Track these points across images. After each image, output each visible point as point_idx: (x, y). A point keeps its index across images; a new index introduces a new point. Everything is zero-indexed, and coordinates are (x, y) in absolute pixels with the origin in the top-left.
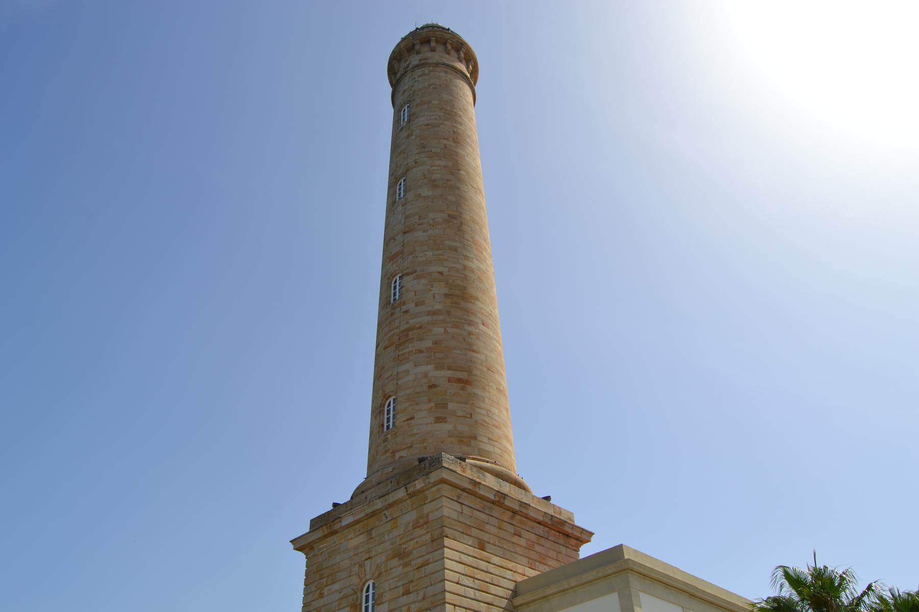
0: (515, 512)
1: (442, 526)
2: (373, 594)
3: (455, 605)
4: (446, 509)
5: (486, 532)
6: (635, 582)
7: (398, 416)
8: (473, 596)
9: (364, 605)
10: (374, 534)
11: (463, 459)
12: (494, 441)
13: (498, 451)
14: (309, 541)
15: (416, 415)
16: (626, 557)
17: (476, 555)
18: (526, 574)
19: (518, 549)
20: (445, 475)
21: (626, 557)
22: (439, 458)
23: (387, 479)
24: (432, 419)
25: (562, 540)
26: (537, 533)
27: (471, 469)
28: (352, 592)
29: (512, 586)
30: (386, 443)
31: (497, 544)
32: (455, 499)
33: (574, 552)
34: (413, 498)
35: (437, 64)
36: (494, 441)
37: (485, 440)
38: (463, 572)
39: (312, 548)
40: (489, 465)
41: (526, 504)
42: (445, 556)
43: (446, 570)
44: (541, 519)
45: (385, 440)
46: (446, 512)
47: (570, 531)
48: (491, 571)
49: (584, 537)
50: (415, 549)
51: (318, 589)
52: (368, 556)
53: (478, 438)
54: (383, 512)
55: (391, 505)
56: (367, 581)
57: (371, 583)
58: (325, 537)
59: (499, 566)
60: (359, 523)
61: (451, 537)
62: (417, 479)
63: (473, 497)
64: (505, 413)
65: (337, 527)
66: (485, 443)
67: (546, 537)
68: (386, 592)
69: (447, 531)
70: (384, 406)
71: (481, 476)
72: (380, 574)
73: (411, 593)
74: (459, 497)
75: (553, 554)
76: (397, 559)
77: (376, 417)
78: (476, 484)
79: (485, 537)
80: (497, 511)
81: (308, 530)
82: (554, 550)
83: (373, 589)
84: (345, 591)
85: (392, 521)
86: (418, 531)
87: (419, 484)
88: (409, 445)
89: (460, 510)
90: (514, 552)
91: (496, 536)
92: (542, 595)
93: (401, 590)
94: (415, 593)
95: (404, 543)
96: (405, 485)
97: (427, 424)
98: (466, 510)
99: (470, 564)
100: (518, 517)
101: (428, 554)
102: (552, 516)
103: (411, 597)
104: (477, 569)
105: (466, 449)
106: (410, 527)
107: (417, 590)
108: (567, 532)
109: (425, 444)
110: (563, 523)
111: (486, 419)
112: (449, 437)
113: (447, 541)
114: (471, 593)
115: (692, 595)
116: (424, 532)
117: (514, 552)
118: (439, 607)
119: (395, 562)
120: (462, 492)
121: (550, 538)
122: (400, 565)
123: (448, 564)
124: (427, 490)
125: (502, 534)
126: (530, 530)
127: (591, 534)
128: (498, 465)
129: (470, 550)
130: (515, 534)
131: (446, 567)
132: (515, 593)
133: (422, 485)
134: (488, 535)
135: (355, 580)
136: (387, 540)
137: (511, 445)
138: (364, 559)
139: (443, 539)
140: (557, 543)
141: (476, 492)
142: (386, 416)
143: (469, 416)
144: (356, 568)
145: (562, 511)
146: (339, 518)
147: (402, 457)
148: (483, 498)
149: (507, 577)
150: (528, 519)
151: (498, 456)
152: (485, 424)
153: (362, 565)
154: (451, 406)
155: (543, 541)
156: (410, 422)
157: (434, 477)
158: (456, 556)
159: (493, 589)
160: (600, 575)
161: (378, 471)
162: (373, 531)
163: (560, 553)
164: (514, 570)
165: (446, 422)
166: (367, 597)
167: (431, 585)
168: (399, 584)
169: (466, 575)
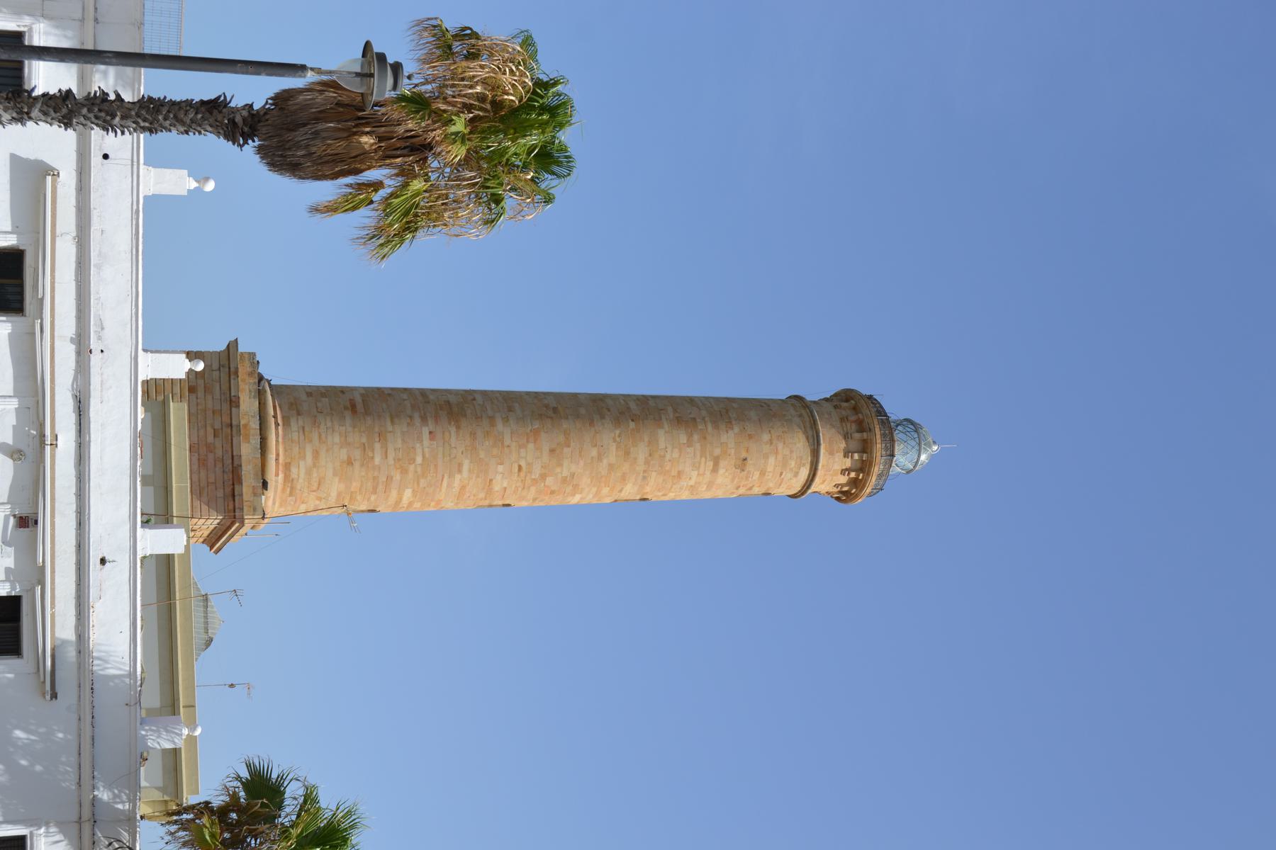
27: (255, 383)
35: (806, 405)
37: (301, 423)
40: (271, 412)
53: (299, 417)
74: (223, 366)
79: (201, 393)
98: (216, 374)
113: (246, 517)
130: (214, 429)
155: (219, 465)
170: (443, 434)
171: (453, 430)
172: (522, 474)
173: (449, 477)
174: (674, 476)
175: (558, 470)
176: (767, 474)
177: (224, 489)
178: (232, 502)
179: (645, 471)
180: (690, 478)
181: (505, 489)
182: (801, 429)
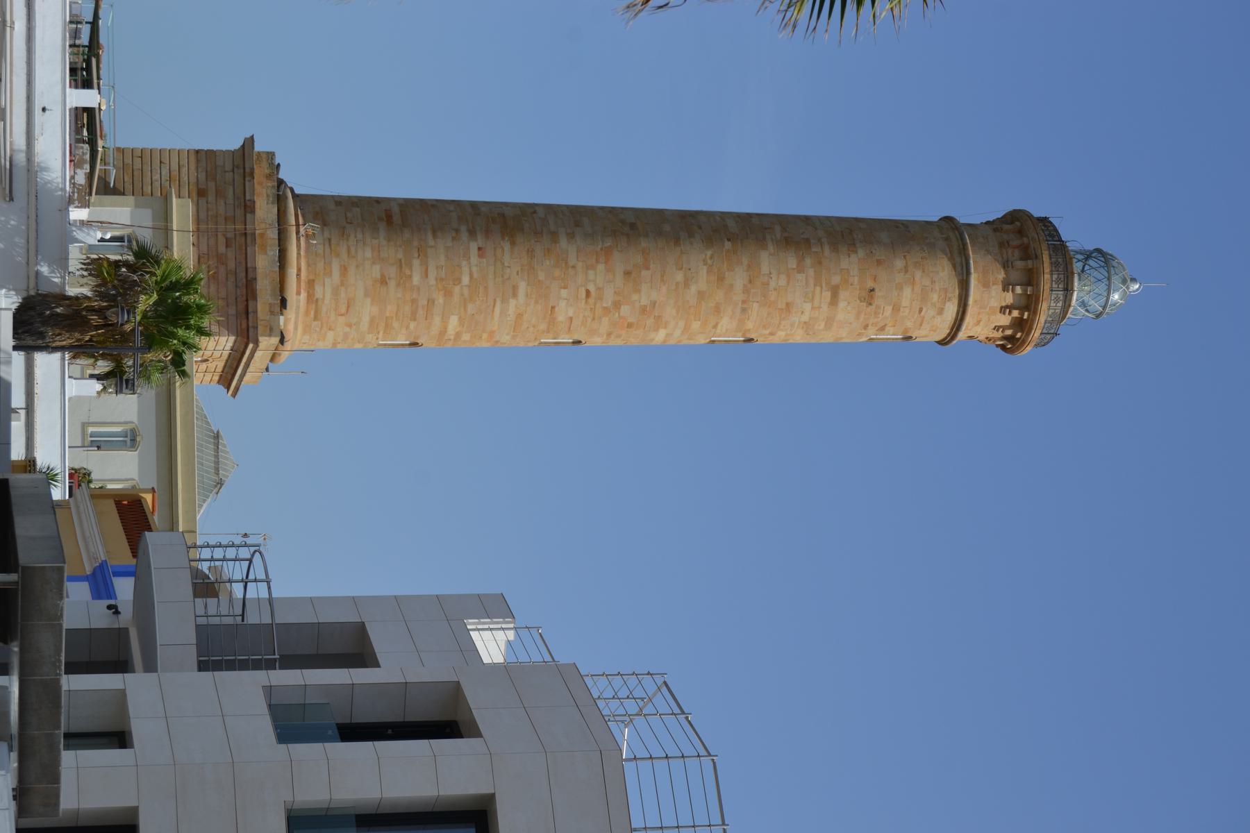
8: (154, 178)
27: (273, 187)
40: (292, 220)
53: (325, 228)
74: (238, 167)
79: (211, 198)
98: (229, 176)
104: (179, 186)
114: (156, 177)
129: (193, 180)
130: (226, 239)
140: (236, 302)
170: (495, 249)
171: (507, 246)
172: (591, 301)
173: (502, 303)
174: (781, 309)
175: (635, 297)
176: (902, 309)
177: (237, 306)
178: (246, 321)
179: (744, 302)
180: (802, 312)
181: (571, 318)
182: (946, 255)
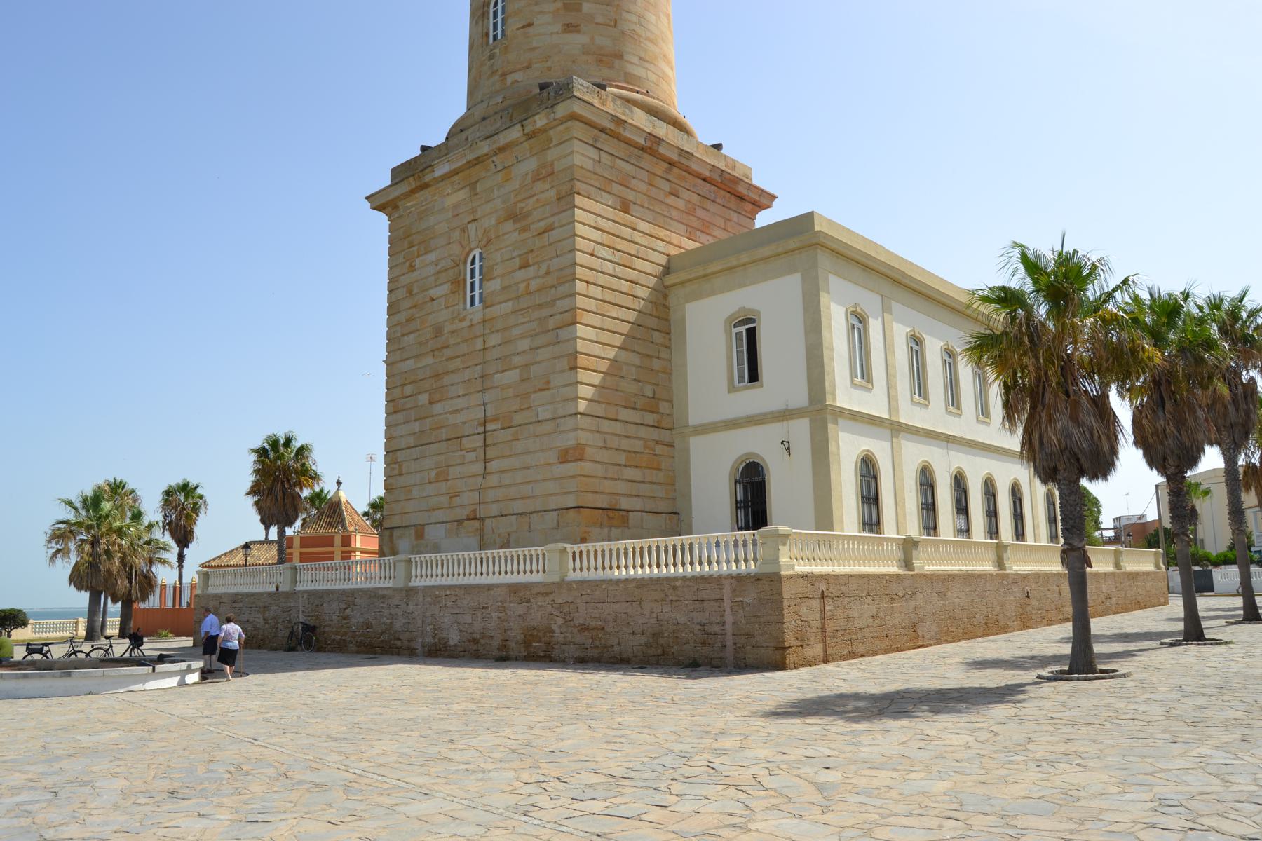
0: (672, 164)
1: (572, 179)
2: (481, 266)
3: (588, 283)
4: (578, 156)
5: (631, 189)
6: (824, 260)
7: (510, 21)
8: (611, 272)
9: (469, 281)
10: (479, 188)
11: (603, 87)
12: (647, 61)
13: (652, 77)
14: (391, 197)
15: (535, 19)
16: (817, 228)
17: (617, 220)
18: (683, 246)
19: (674, 214)
20: (577, 108)
21: (817, 228)
22: (568, 84)
23: (496, 113)
24: (558, 27)
25: (733, 203)
26: (701, 193)
27: (614, 101)
28: (453, 264)
29: (663, 260)
30: (492, 61)
31: (646, 205)
32: (591, 142)
33: (749, 220)
34: (533, 140)
36: (647, 61)
37: (635, 60)
38: (600, 241)
39: (396, 207)
40: (639, 96)
41: (688, 153)
42: (576, 218)
43: (576, 238)
44: (707, 174)
45: (491, 57)
46: (578, 160)
47: (745, 192)
48: (636, 240)
49: (764, 201)
50: (535, 209)
51: (406, 261)
52: (471, 218)
53: (625, 58)
54: (491, 159)
55: (502, 149)
56: (472, 250)
57: (477, 252)
58: (413, 192)
59: (647, 234)
60: (458, 173)
61: (585, 194)
62: (537, 114)
63: (615, 141)
64: (664, 19)
65: (428, 178)
66: (635, 64)
67: (712, 198)
68: (497, 264)
69: (580, 186)
70: (488, 7)
71: (627, 111)
72: (489, 241)
73: (530, 266)
74: (595, 141)
75: (721, 222)
76: (511, 221)
77: (477, 23)
78: (620, 122)
79: (631, 196)
80: (647, 161)
81: (389, 183)
82: (721, 217)
83: (481, 261)
84: (442, 264)
85: (504, 172)
86: (540, 186)
87: (540, 121)
88: (525, 65)
89: (597, 158)
90: (667, 217)
91: (645, 195)
92: (702, 273)
93: (517, 262)
94: (536, 266)
95: (523, 200)
96: (522, 121)
97: (552, 33)
99: (607, 230)
100: (676, 170)
101: (553, 215)
102: (722, 171)
103: (531, 271)
104: (618, 237)
105: (606, 72)
106: (529, 180)
107: (537, 263)
108: (740, 193)
109: (549, 64)
110: (737, 180)
111: (637, 29)
112: (583, 53)
113: (578, 200)
114: (609, 267)
115: (897, 282)
116: (547, 186)
117: (667, 217)
118: (567, 285)
119: (509, 226)
120: (599, 133)
121: (718, 200)
122: (515, 230)
123: (580, 229)
124: (551, 129)
125: (653, 192)
126: (691, 189)
127: (774, 197)
128: (651, 97)
129: (610, 213)
131: (577, 233)
132: (667, 270)
133: (544, 121)
134: (634, 193)
135: (456, 249)
136: (499, 197)
137: (672, 69)
138: (466, 222)
139: (574, 197)
140: (727, 207)
141: (620, 134)
142: (492, 21)
143: (612, 23)
144: (456, 235)
145: (737, 165)
146: (431, 166)
147: (516, 81)
148: (628, 142)
149: (658, 249)
150: (689, 173)
151: (652, 85)
152: (636, 37)
153: (463, 230)
154: (587, 7)
155: (707, 204)
156: (530, 30)
157: (561, 110)
158: (591, 219)
159: (638, 264)
160: (780, 250)
161: (482, 101)
162: (478, 184)
163: (730, 220)
164: (668, 240)
165: (578, 32)
166: (473, 271)
167: (557, 256)
168: (515, 254)
169: (604, 245)
